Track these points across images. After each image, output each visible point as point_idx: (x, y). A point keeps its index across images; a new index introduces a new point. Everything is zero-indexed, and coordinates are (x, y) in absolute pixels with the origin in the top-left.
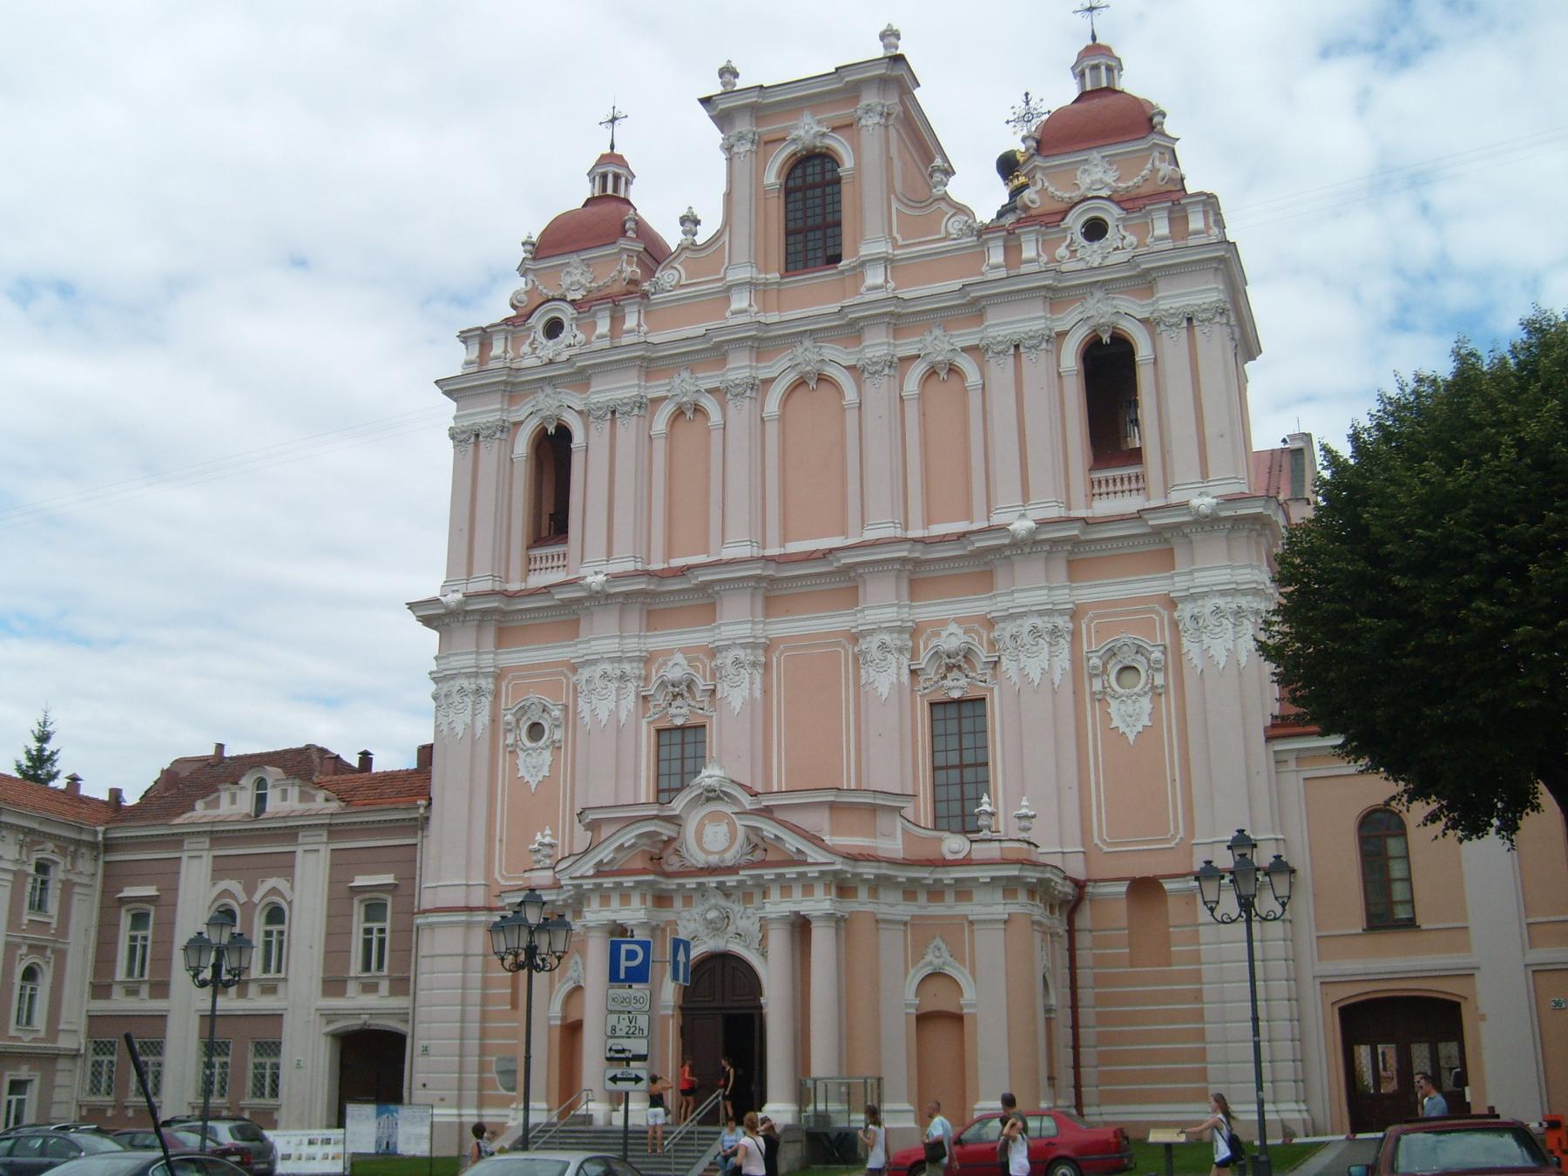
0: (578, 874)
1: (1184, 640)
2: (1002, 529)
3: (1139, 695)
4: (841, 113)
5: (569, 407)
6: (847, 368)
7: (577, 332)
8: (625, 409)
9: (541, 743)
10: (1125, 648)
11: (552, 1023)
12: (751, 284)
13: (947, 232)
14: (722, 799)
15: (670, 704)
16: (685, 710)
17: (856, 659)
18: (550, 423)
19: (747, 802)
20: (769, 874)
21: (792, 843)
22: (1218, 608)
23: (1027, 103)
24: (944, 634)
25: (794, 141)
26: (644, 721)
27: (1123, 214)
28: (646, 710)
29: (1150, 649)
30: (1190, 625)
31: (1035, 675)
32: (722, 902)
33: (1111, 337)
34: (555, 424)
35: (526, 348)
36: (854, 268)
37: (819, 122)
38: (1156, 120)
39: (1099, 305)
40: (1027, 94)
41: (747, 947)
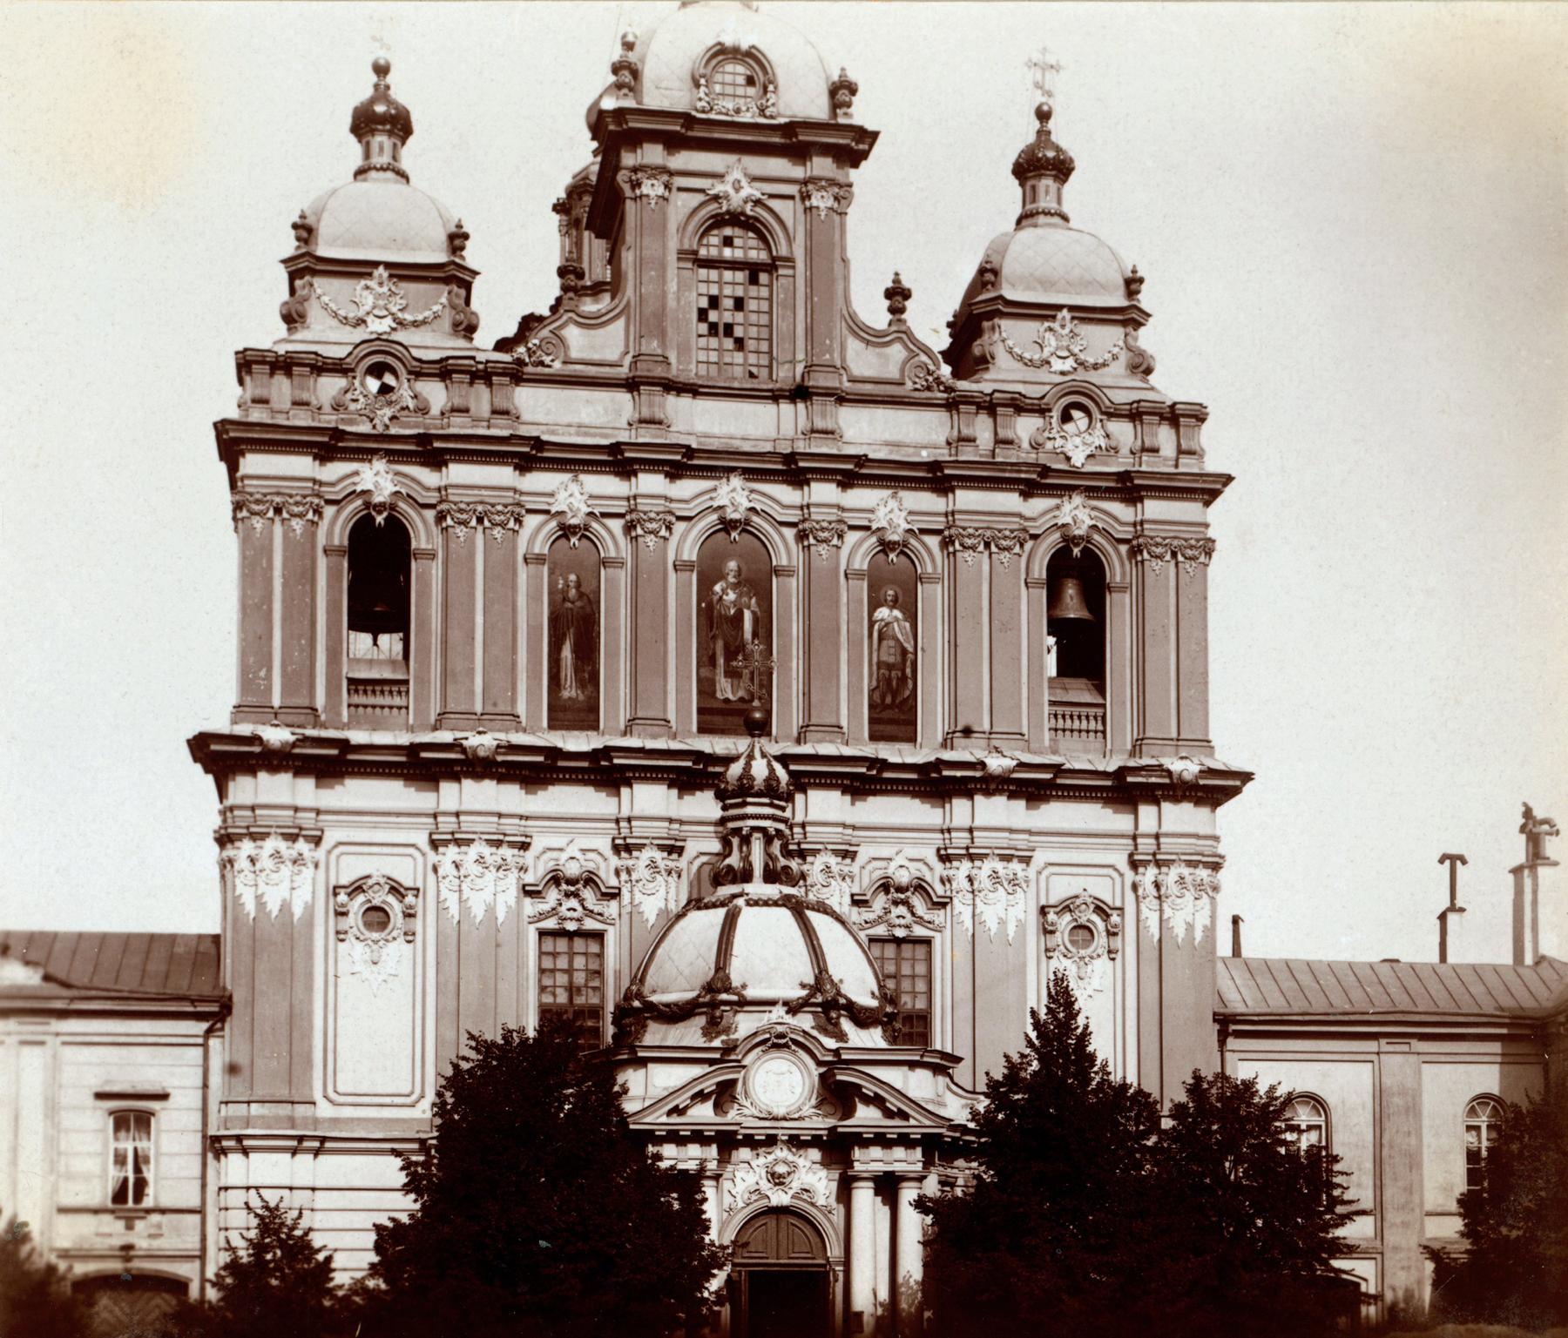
1: (1143, 906)
3: (1092, 958)
5: (408, 495)
10: (1084, 907)
14: (789, 1047)
15: (561, 905)
16: (575, 915)
18: (380, 513)
22: (1182, 878)
24: (893, 865)
29: (1109, 911)
30: (1152, 891)
31: (993, 925)
32: (790, 1158)
33: (1081, 551)
34: (385, 514)
39: (1076, 512)
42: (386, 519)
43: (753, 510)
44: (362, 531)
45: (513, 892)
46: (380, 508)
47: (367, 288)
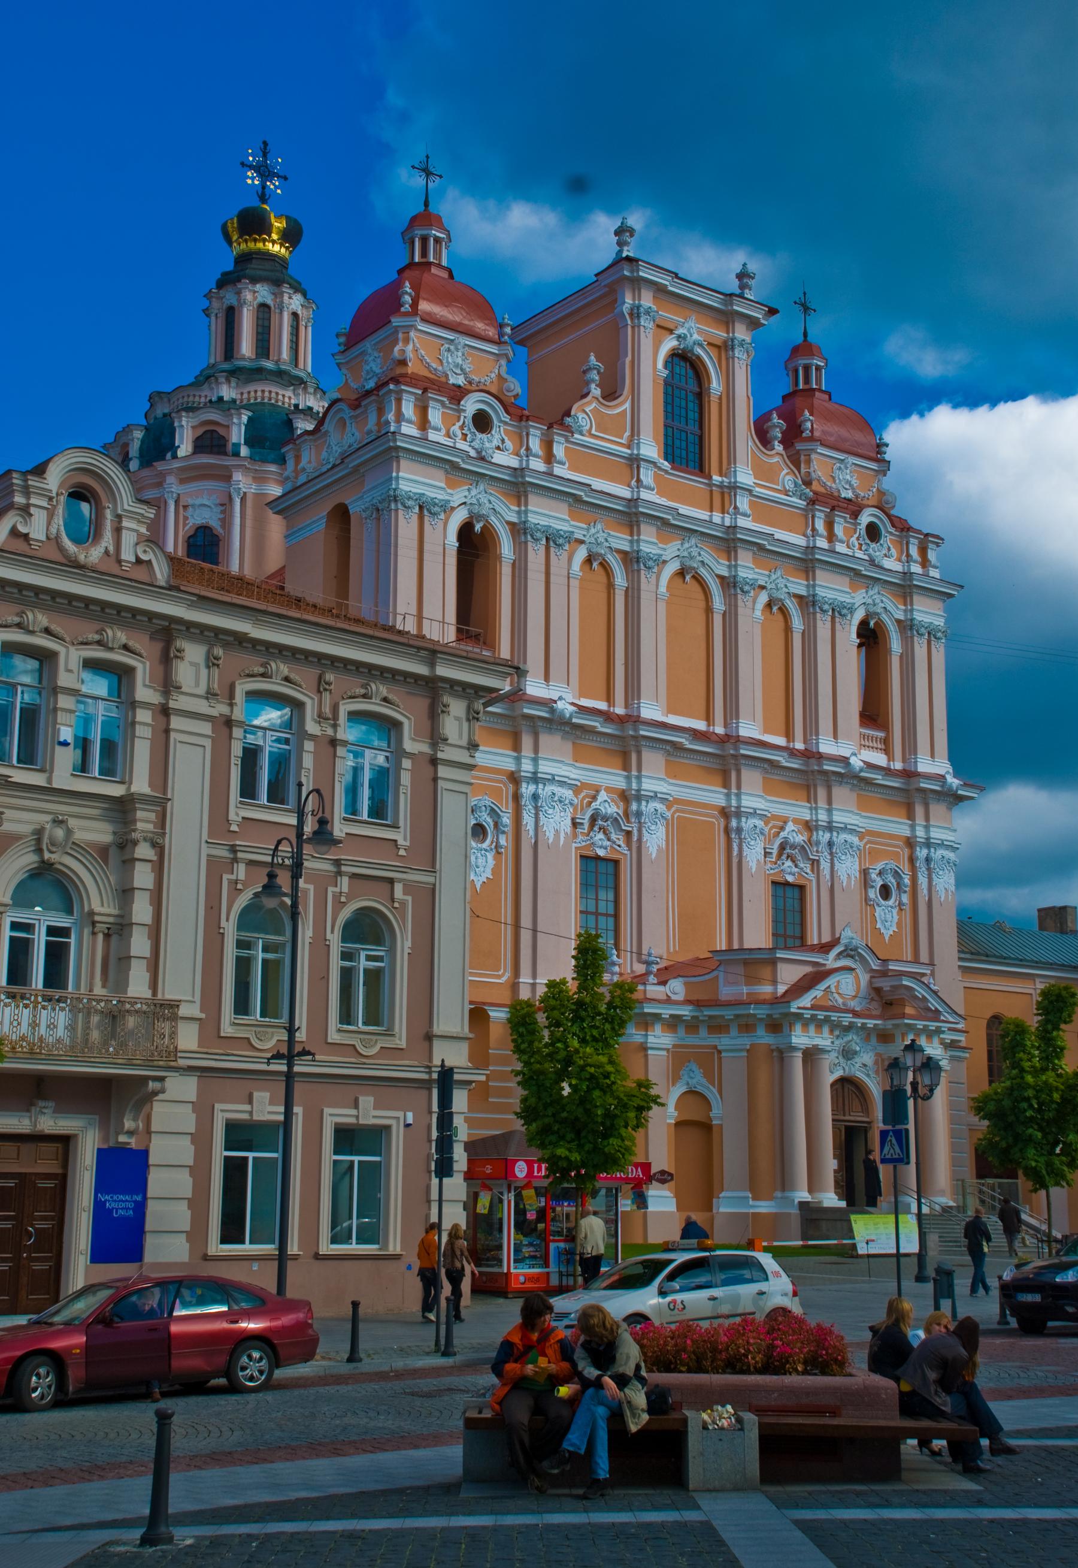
0: (801, 1005)
2: (845, 761)
4: (719, 334)
6: (718, 576)
7: (506, 438)
8: (561, 541)
9: (485, 845)
11: (669, 1121)
12: (654, 463)
13: (784, 487)
17: (727, 831)
18: (478, 522)
19: (875, 965)
20: (920, 1024)
21: (934, 1004)
23: (265, 155)
25: (679, 337)
26: (574, 845)
27: (892, 530)
28: (575, 836)
35: (456, 428)
36: (721, 486)
37: (700, 332)
38: (884, 449)
40: (265, 144)
41: (868, 1075)
42: (482, 528)
43: (702, 562)
44: (466, 532)
45: (569, 822)
46: (480, 517)
47: (449, 350)
